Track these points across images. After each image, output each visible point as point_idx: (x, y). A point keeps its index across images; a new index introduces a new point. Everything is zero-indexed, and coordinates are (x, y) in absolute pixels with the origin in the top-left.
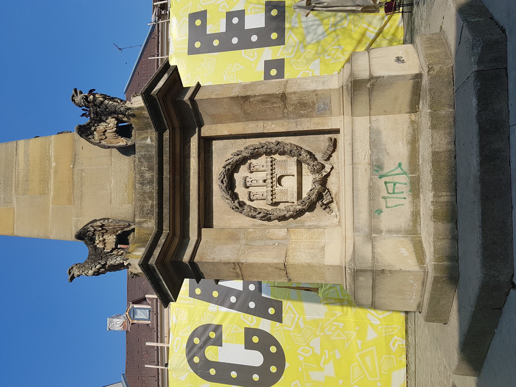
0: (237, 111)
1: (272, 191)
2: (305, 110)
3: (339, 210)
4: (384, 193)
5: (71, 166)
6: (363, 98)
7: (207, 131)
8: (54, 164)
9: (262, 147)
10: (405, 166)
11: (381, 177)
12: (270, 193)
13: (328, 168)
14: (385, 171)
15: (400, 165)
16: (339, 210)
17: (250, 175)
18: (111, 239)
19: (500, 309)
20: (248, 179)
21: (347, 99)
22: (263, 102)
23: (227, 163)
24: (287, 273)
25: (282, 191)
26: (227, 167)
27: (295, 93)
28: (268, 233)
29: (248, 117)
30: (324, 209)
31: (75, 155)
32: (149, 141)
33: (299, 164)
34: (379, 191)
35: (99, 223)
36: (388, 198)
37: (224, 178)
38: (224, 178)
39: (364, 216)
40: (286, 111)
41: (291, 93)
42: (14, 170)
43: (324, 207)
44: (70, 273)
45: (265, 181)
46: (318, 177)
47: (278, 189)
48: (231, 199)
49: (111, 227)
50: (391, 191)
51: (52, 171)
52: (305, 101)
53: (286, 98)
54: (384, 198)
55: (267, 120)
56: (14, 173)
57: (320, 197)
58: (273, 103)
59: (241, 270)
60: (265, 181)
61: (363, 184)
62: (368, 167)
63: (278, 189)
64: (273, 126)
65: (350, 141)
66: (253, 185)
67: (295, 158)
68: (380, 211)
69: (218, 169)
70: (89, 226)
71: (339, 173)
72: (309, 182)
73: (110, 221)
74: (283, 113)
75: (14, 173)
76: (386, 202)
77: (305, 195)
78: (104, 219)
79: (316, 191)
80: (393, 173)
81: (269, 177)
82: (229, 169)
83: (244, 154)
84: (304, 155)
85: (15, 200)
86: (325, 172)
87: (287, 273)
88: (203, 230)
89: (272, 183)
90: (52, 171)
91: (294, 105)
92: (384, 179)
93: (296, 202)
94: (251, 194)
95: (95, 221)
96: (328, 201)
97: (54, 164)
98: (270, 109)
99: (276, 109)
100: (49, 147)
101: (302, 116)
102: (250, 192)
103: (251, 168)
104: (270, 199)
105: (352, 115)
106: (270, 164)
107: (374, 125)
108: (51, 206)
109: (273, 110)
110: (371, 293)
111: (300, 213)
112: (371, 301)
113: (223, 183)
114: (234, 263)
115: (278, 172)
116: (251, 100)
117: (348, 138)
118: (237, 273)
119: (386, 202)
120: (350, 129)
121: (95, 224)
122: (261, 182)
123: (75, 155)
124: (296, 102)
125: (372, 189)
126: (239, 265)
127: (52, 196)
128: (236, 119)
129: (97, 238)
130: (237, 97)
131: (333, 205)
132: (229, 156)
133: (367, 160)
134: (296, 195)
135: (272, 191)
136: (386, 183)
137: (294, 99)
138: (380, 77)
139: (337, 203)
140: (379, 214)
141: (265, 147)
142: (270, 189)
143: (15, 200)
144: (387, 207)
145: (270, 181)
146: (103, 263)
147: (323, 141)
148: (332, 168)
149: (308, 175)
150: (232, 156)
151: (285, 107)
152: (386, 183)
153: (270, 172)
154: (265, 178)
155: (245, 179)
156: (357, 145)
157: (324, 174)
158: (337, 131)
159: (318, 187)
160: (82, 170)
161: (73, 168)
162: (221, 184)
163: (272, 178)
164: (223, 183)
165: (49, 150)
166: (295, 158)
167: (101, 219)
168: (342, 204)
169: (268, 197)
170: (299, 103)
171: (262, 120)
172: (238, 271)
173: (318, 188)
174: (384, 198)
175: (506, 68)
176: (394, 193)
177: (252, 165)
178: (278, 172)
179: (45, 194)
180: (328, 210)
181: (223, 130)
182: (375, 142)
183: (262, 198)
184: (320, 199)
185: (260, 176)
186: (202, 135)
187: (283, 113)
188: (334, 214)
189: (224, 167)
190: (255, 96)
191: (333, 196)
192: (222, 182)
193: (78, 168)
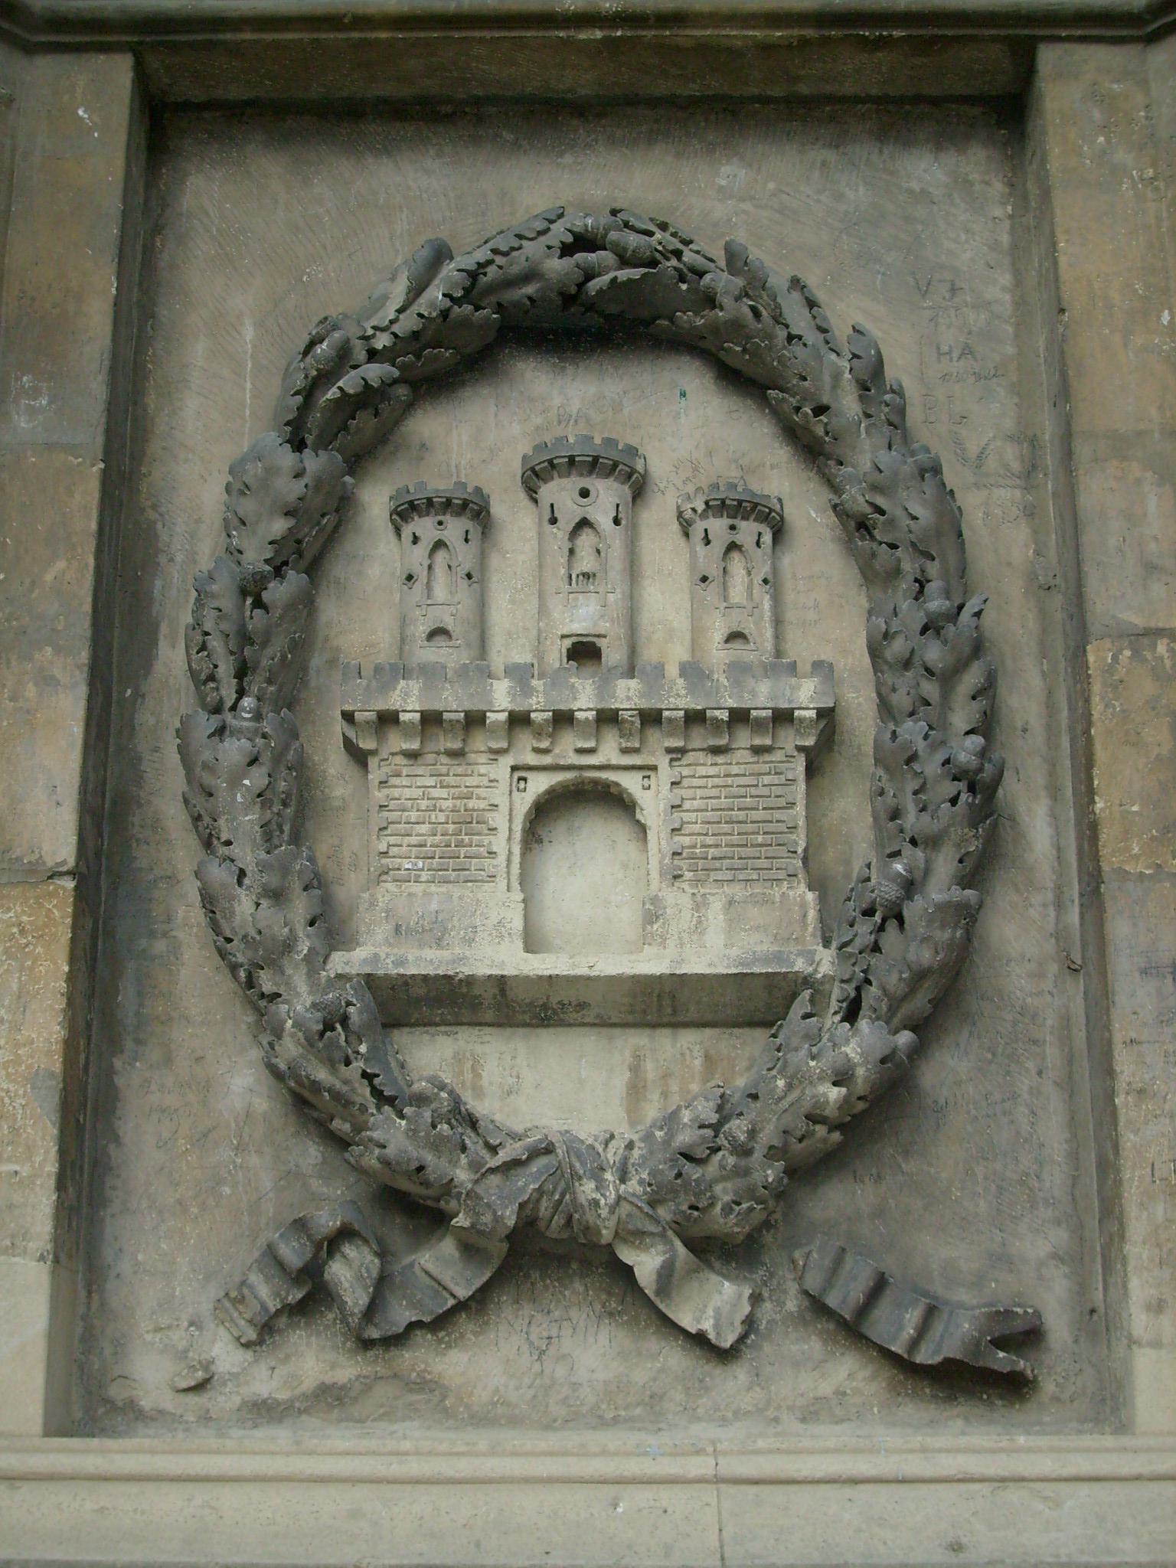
1: (474, 720)
3: (264, 1411)
12: (452, 701)
13: (714, 1303)
20: (607, 494)
23: (778, 281)
25: (469, 822)
28: (46, 681)
30: (271, 1256)
33: (757, 1003)
37: (625, 260)
38: (625, 260)
46: (600, 1197)
48: (408, 324)
69: (727, 203)
72: (567, 1103)
79: (463, 1176)
81: (627, 695)
84: (852, 1050)
86: (666, 1277)
88: (117, 74)
89: (563, 719)
93: (348, 961)
103: (718, 525)
104: (393, 701)
113: (567, 250)
131: (313, 1358)
134: (423, 961)
135: (474, 720)
142: (501, 698)
145: (585, 711)
147: (1002, 1259)
149: (636, 1091)
150: (841, 332)
153: (678, 699)
157: (646, 1263)
162: (559, 233)
163: (607, 718)
164: (567, 250)
168: (337, 1448)
169: (415, 686)
177: (748, 530)
186: (1048, 57)
188: (224, 1353)
189: (735, 260)
191: (419, 1357)
192: (582, 242)
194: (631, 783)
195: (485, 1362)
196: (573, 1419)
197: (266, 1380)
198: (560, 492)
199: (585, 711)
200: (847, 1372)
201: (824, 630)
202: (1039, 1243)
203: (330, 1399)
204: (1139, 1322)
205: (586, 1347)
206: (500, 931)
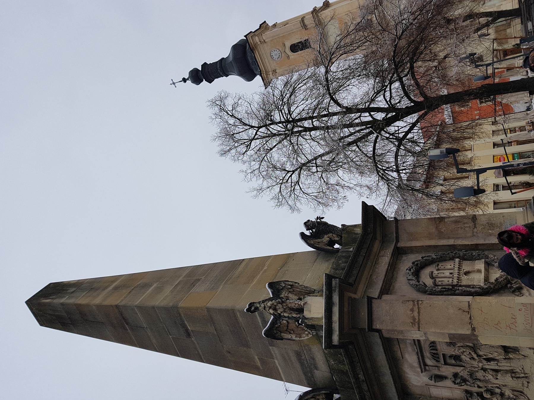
0: (432, 229)
8: (265, 268)
24: (470, 318)
29: (441, 235)
32: (351, 249)
35: (290, 283)
40: (475, 230)
52: (493, 222)
58: (464, 223)
59: (419, 313)
87: (470, 318)
91: (483, 225)
95: (288, 281)
97: (265, 268)
98: (461, 228)
99: (467, 229)
109: (464, 229)
116: (446, 220)
118: (414, 319)
121: (287, 283)
124: (485, 223)
126: (418, 304)
128: (430, 236)
129: (284, 293)
151: (475, 227)
166: (484, 260)
170: (488, 223)
171: (453, 238)
172: (416, 314)
193: (284, 269)
198: (434, 275)
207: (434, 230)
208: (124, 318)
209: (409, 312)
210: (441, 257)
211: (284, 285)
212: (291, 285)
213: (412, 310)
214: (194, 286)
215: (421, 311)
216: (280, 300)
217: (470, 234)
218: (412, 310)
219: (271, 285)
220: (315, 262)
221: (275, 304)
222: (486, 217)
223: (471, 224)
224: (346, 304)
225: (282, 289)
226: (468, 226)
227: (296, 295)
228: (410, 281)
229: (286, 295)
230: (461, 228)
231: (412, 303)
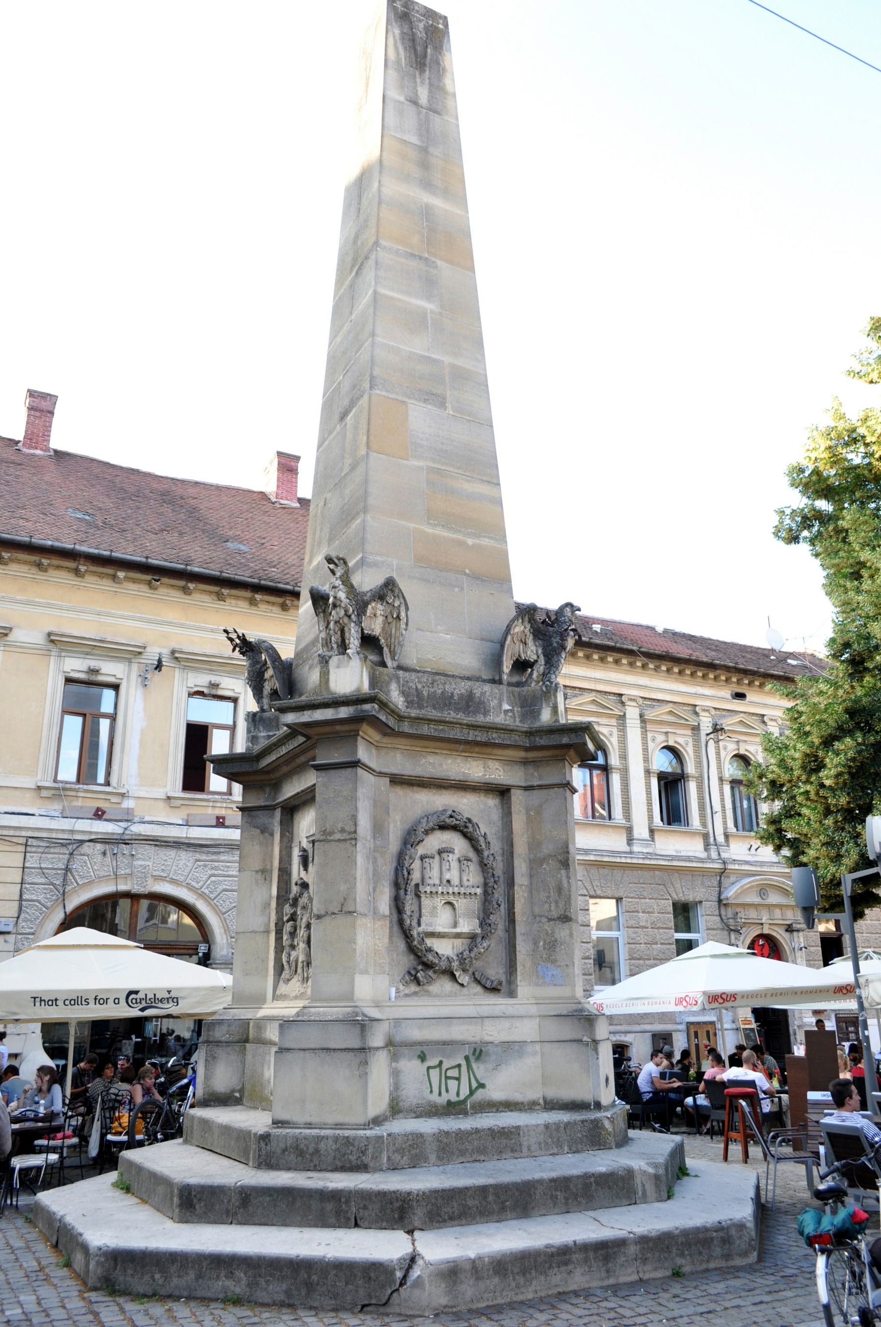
0: (547, 848)
2: (544, 948)
3: (407, 995)
4: (445, 1066)
5: (467, 571)
6: (568, 1030)
7: (517, 797)
8: (470, 542)
9: (495, 882)
10: (480, 1095)
11: (467, 1058)
12: (434, 890)
14: (474, 1065)
15: (482, 1086)
16: (407, 995)
17: (456, 856)
18: (375, 627)
19: (356, 1225)
20: (451, 855)
21: (564, 1009)
22: (559, 889)
24: (334, 913)
25: (435, 908)
26: (470, 825)
27: (571, 935)
28: (383, 886)
29: (535, 864)
31: (483, 580)
34: (449, 1057)
35: (403, 614)
36: (441, 1070)
39: (416, 1034)
40: (544, 920)
41: (570, 929)
42: (460, 472)
43: (413, 972)
44: (339, 559)
45: (448, 881)
47: (439, 902)
49: (393, 631)
50: (449, 1073)
51: (459, 537)
52: (557, 950)
53: (564, 922)
54: (441, 1063)
55: (531, 892)
56: (456, 471)
57: (428, 966)
58: (557, 902)
59: (339, 840)
60: (448, 881)
61: (458, 1032)
62: (477, 1039)
63: (439, 902)
64: (523, 900)
65: (507, 1014)
66: (444, 862)
67: (479, 931)
68: (423, 1058)
70: (402, 601)
71: (456, 996)
72: (445, 949)
73: (404, 632)
74: (541, 916)
75: (456, 471)
76: (434, 1067)
77: (429, 942)
78: (407, 624)
80: (472, 1076)
81: (456, 890)
82: (466, 827)
83: (486, 853)
85: (421, 463)
87: (334, 913)
88: (388, 780)
90: (459, 537)
92: (463, 1063)
94: (431, 860)
95: (407, 609)
96: (421, 979)
97: (470, 542)
98: (548, 897)
99: (546, 906)
100: (491, 538)
101: (536, 944)
102: (433, 858)
103: (465, 862)
105: (540, 1016)
106: (473, 891)
107: (530, 1048)
108: (412, 525)
109: (546, 902)
110: (312, 1046)
111: (407, 935)
112: (292, 1046)
114: (355, 832)
115: (461, 904)
116: (563, 872)
117: (497, 1011)
118: (332, 833)
119: (434, 1067)
120: (523, 1013)
121: (403, 608)
122: (447, 876)
123: (483, 580)
124: (557, 936)
125: (445, 1044)
126: (351, 839)
127: (427, 530)
128: (534, 845)
130: (568, 852)
131: (413, 988)
132: (483, 829)
133: (488, 1038)
134: (430, 929)
136: (459, 1066)
137: (562, 932)
138: (597, 1053)
139: (415, 993)
140: (419, 1057)
141: (496, 886)
142: (440, 890)
143: (421, 463)
144: (429, 1068)
146: (353, 616)
148: (462, 985)
149: (453, 948)
151: (550, 920)
152: (459, 1066)
154: (452, 883)
155: (451, 851)
156: (506, 1024)
157: (457, 974)
158: (512, 994)
159: (444, 965)
160: (462, 589)
161: (465, 574)
165: (489, 538)
167: (407, 620)
170: (556, 941)
172: (338, 836)
173: (441, 963)
174: (441, 1063)
175: (635, 1203)
176: (447, 1078)
178: (461, 904)
179: (429, 519)
180: (407, 978)
181: (519, 822)
182: (511, 1049)
183: (427, 877)
184: (421, 965)
185: (453, 875)
187: (541, 916)
188: (401, 987)
189: (469, 820)
190: (568, 877)
194: (455, 902)
195: (434, 988)
196: (445, 996)
197: (407, 992)
198: (444, 855)
199: (451, 891)
200: (479, 989)
201: (473, 877)
202: (501, 970)
203: (415, 993)
204: (519, 983)
205: (444, 985)
206: (439, 925)
207: (546, 851)
208: (361, 265)
209: (340, 825)
210: (486, 865)
211: (396, 605)
212: (398, 617)
213: (343, 831)
214: (425, 401)
215: (341, 845)
216: (351, 610)
217: (537, 910)
218: (343, 831)
219: (390, 585)
220: (482, 639)
221: (343, 605)
222: (567, 938)
223: (555, 914)
224: (346, 728)
225: (387, 603)
226: (552, 908)
227: (383, 629)
228: (426, 819)
229: (379, 613)
230: (548, 897)
231: (353, 830)
